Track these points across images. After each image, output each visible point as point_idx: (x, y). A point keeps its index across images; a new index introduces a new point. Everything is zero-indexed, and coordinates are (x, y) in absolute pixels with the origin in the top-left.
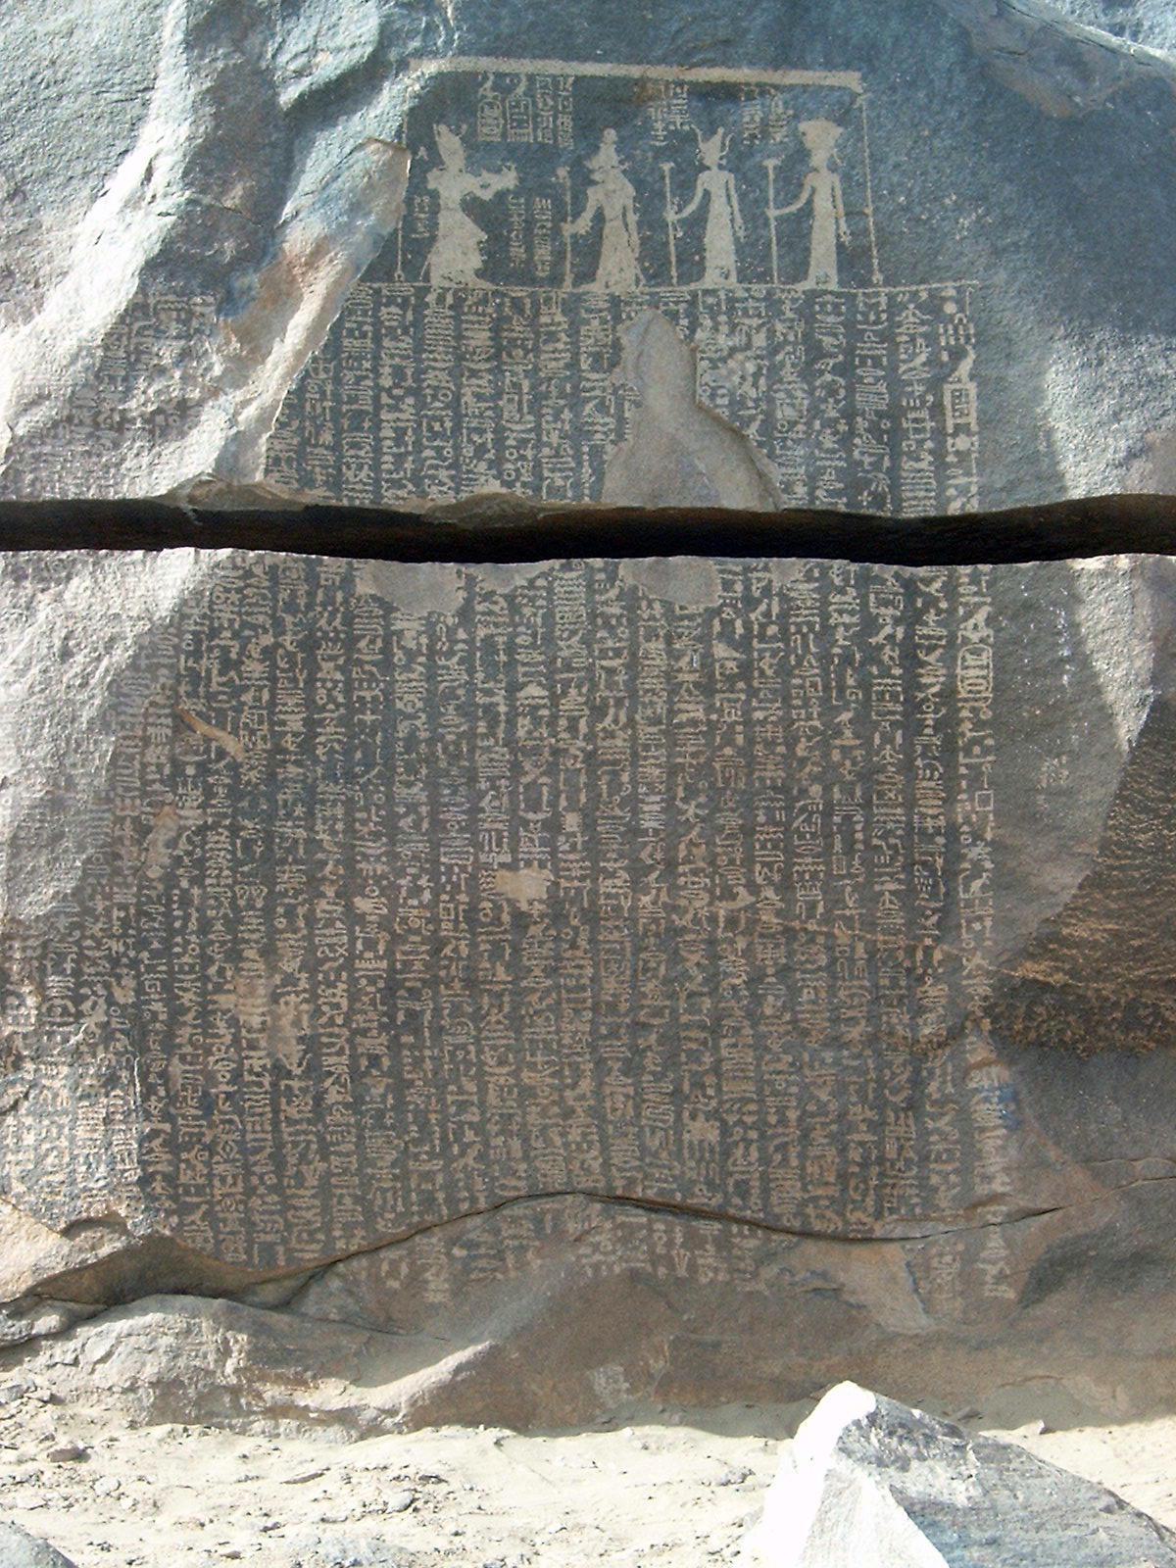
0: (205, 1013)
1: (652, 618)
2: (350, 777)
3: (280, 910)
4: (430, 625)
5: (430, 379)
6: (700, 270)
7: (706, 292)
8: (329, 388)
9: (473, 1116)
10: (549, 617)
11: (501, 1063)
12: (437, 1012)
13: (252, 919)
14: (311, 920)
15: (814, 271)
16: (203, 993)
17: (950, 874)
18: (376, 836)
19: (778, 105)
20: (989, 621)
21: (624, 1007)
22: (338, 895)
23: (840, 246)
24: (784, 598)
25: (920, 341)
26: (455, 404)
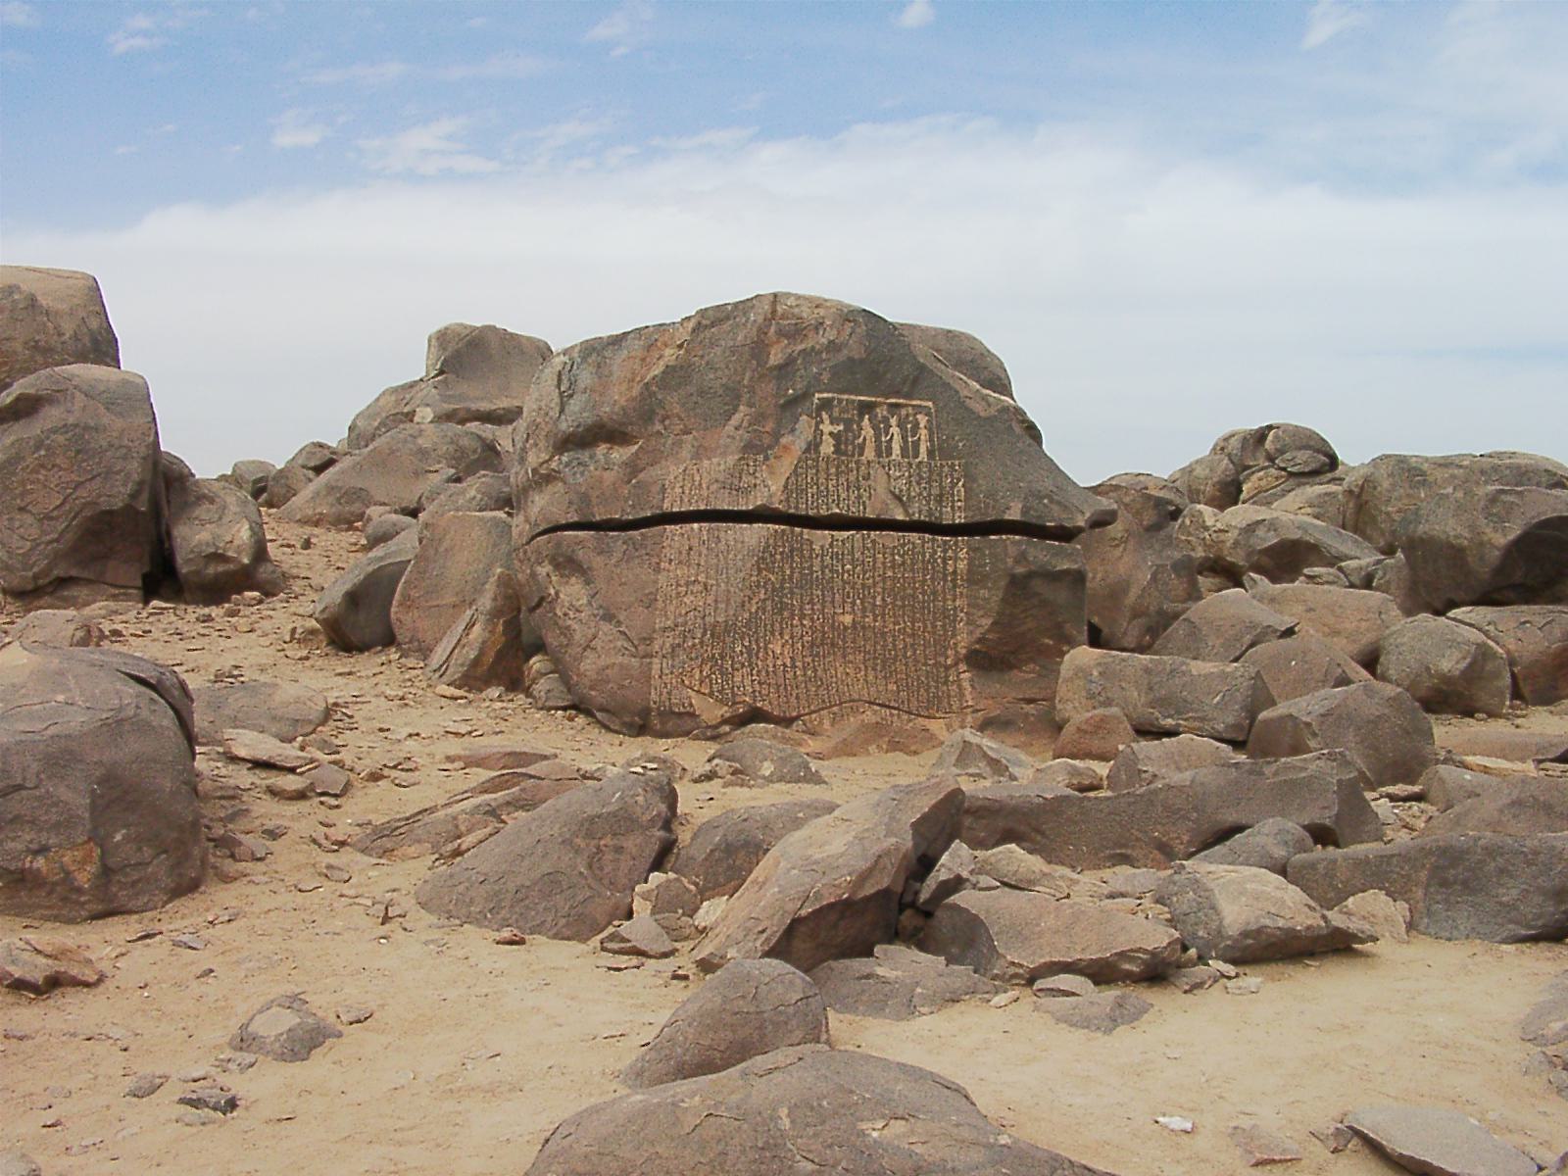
0: (766, 648)
2: (802, 588)
4: (822, 547)
9: (834, 680)
17: (954, 621)
24: (913, 543)
26: (827, 488)
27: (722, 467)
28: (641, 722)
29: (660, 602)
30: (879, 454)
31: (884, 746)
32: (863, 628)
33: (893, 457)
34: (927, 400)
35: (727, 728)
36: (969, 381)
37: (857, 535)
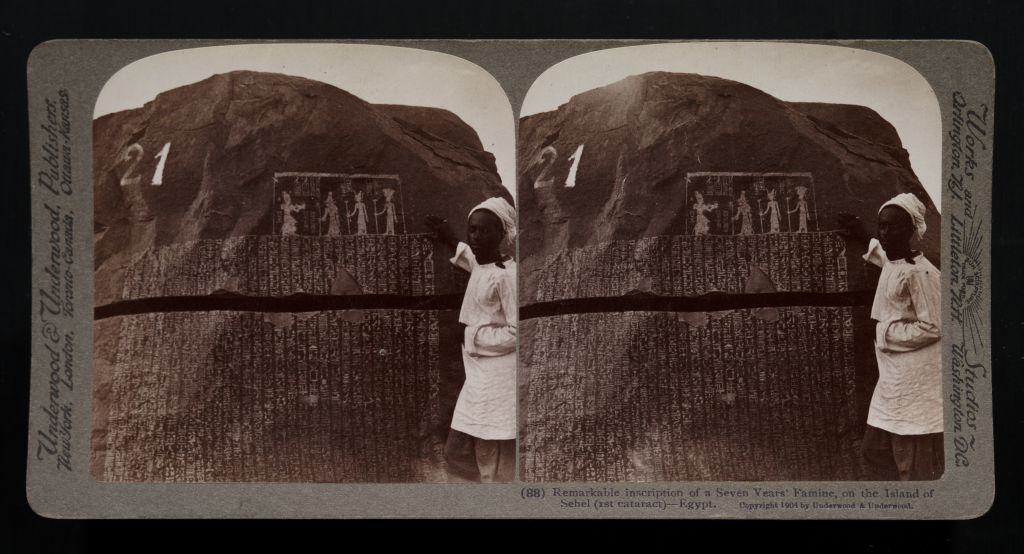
0: (223, 438)
6: (356, 230)
10: (317, 326)
11: (305, 447)
14: (252, 411)
23: (395, 223)
27: (181, 253)
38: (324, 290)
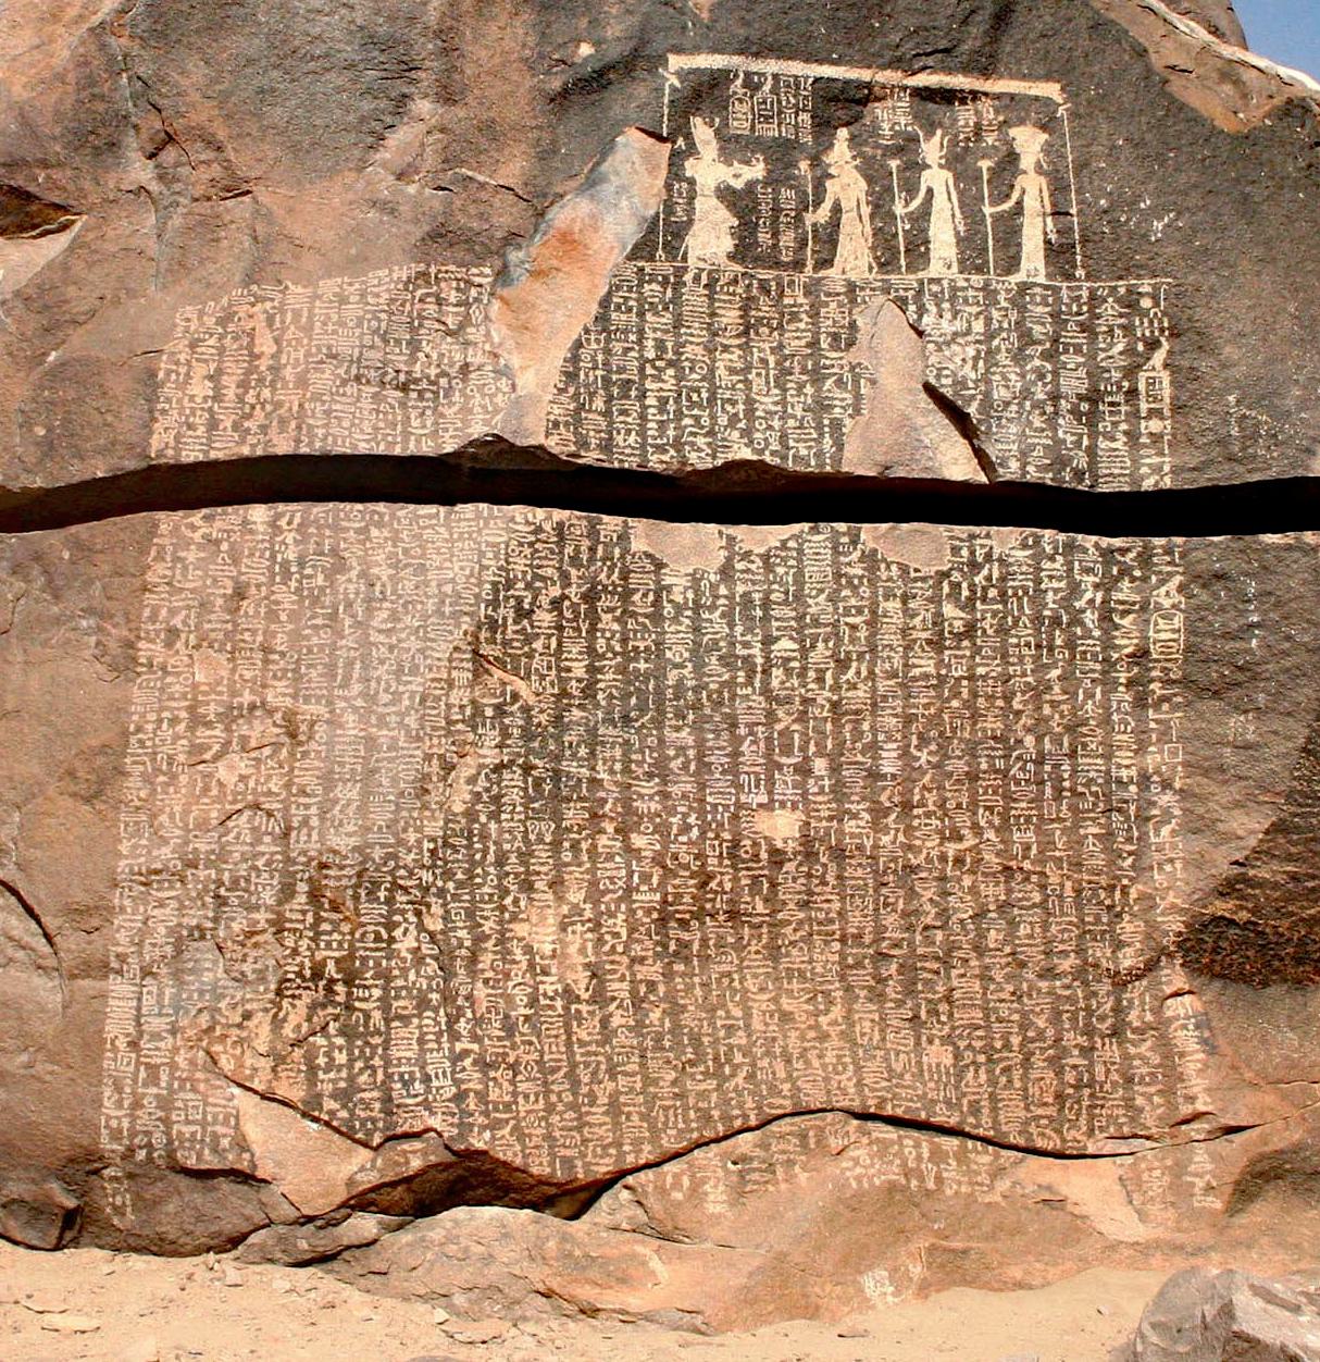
0: (502, 941)
1: (890, 579)
2: (626, 720)
3: (566, 844)
4: (695, 579)
5: (690, 351)
6: (925, 257)
7: (931, 281)
8: (600, 358)
9: (740, 1039)
10: (799, 575)
11: (762, 990)
12: (704, 942)
13: (542, 853)
15: (1024, 264)
16: (501, 922)
18: (650, 776)
19: (987, 110)
20: (1181, 589)
21: (867, 939)
22: (617, 831)
23: (1047, 242)
25: (1117, 331)
26: (710, 376)
27: (353, 310)
28: (71, 1203)
29: (133, 782)
30: (886, 264)
31: (917, 1270)
32: (839, 854)
33: (935, 269)
34: (1048, 78)
35: (365, 1225)
36: (1174, 17)
37: (814, 541)
38: (819, 455)
